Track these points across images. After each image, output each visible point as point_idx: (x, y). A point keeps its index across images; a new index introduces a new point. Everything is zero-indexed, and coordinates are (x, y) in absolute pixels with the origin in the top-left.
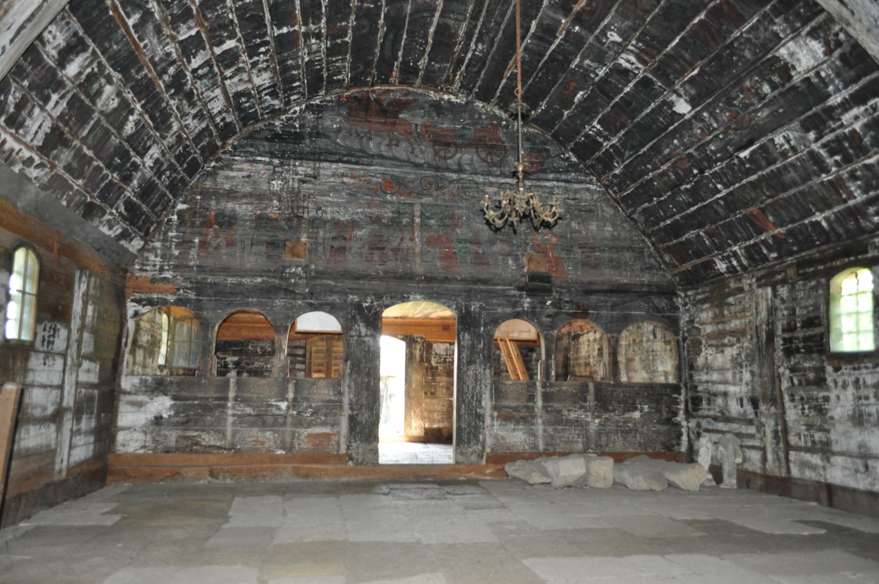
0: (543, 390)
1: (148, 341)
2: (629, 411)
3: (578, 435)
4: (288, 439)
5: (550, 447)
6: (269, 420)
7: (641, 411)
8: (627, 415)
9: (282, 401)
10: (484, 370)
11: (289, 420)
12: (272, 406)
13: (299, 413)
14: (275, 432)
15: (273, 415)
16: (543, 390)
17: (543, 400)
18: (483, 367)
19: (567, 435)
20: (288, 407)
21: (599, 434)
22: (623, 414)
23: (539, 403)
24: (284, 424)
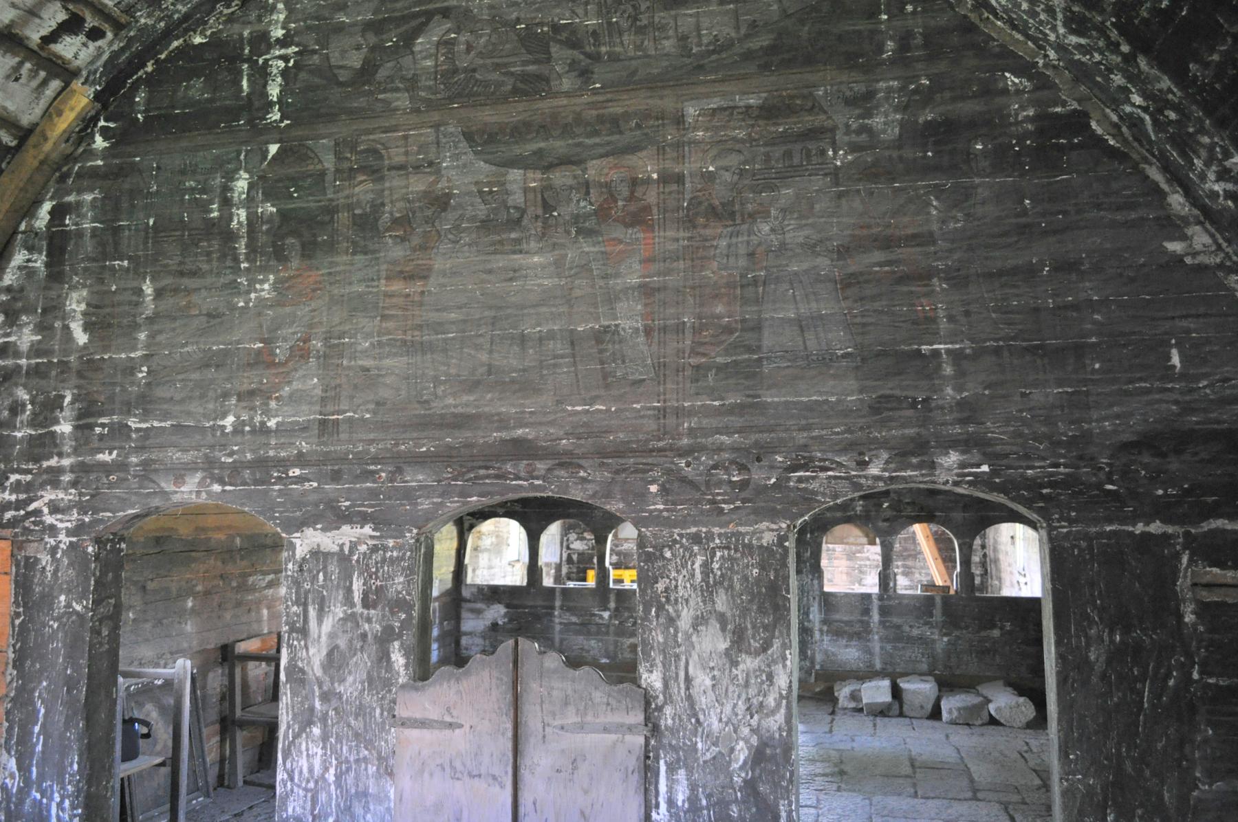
0: (880, 603)
1: (492, 544)
2: (985, 628)
3: (923, 654)
4: (611, 648)
5: (888, 666)
6: (593, 629)
7: (1001, 629)
8: (983, 634)
9: (605, 610)
10: (812, 580)
11: (612, 628)
12: (595, 615)
13: (621, 623)
14: (599, 641)
15: (597, 624)
16: (880, 603)
17: (880, 615)
18: (810, 577)
19: (908, 654)
20: (610, 617)
21: (948, 654)
22: (978, 632)
23: (876, 617)
24: (607, 633)
